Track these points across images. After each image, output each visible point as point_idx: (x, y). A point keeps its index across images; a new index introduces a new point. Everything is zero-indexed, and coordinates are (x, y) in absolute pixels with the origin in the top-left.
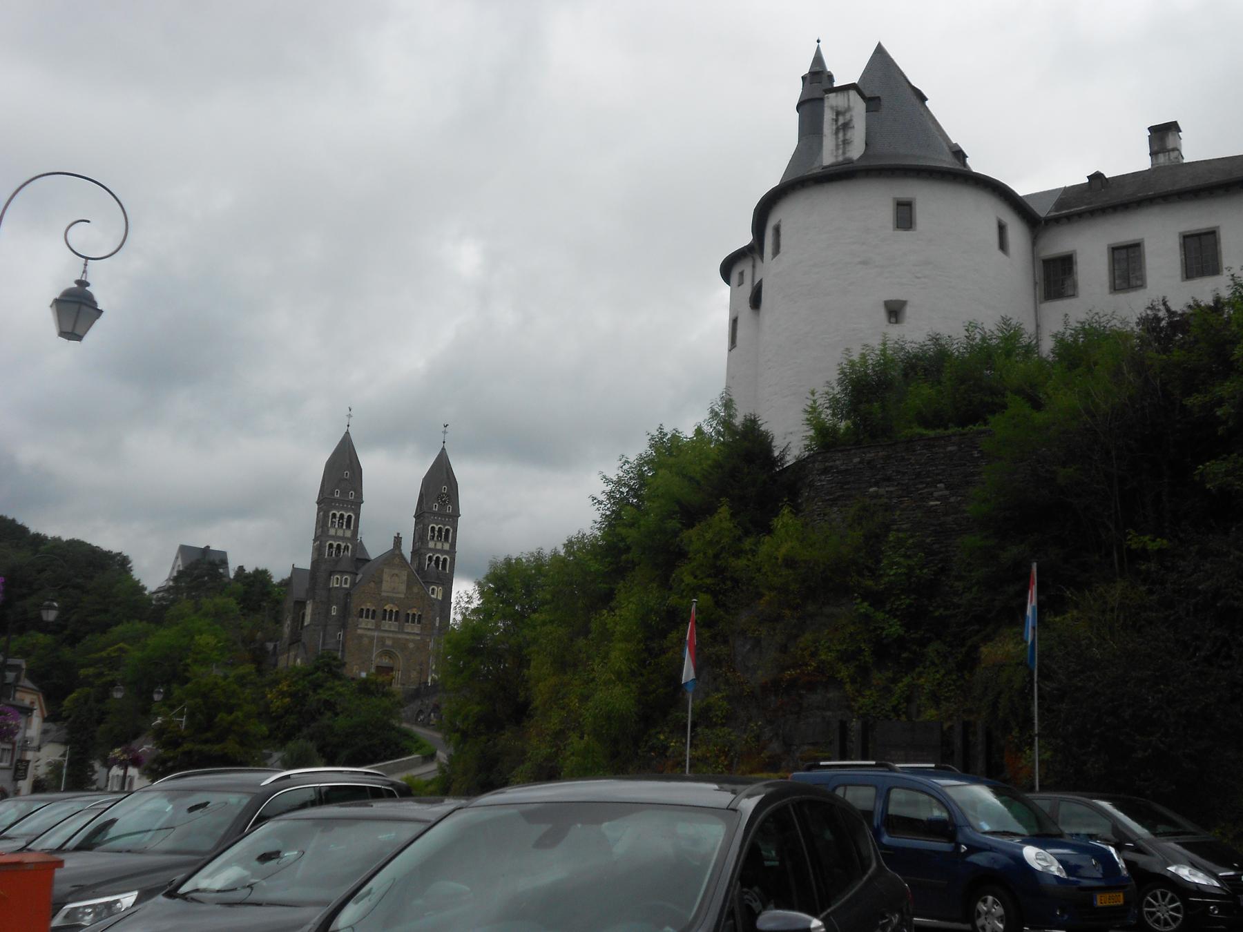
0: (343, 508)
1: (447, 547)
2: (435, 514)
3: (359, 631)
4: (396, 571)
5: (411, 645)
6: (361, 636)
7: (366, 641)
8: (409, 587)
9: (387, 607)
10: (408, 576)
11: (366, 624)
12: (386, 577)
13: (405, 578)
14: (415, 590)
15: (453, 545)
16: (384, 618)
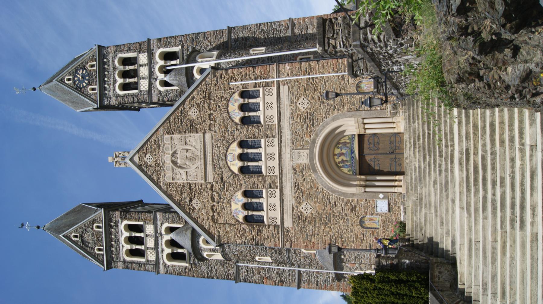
0: (117, 241)
1: (143, 58)
2: (102, 89)
3: (288, 223)
4: (167, 159)
5: (303, 104)
6: (299, 218)
7: (306, 209)
8: (192, 128)
9: (235, 165)
10: (170, 132)
11: (271, 209)
12: (181, 178)
13: (176, 136)
14: (193, 114)
15: (141, 47)
16: (258, 172)
